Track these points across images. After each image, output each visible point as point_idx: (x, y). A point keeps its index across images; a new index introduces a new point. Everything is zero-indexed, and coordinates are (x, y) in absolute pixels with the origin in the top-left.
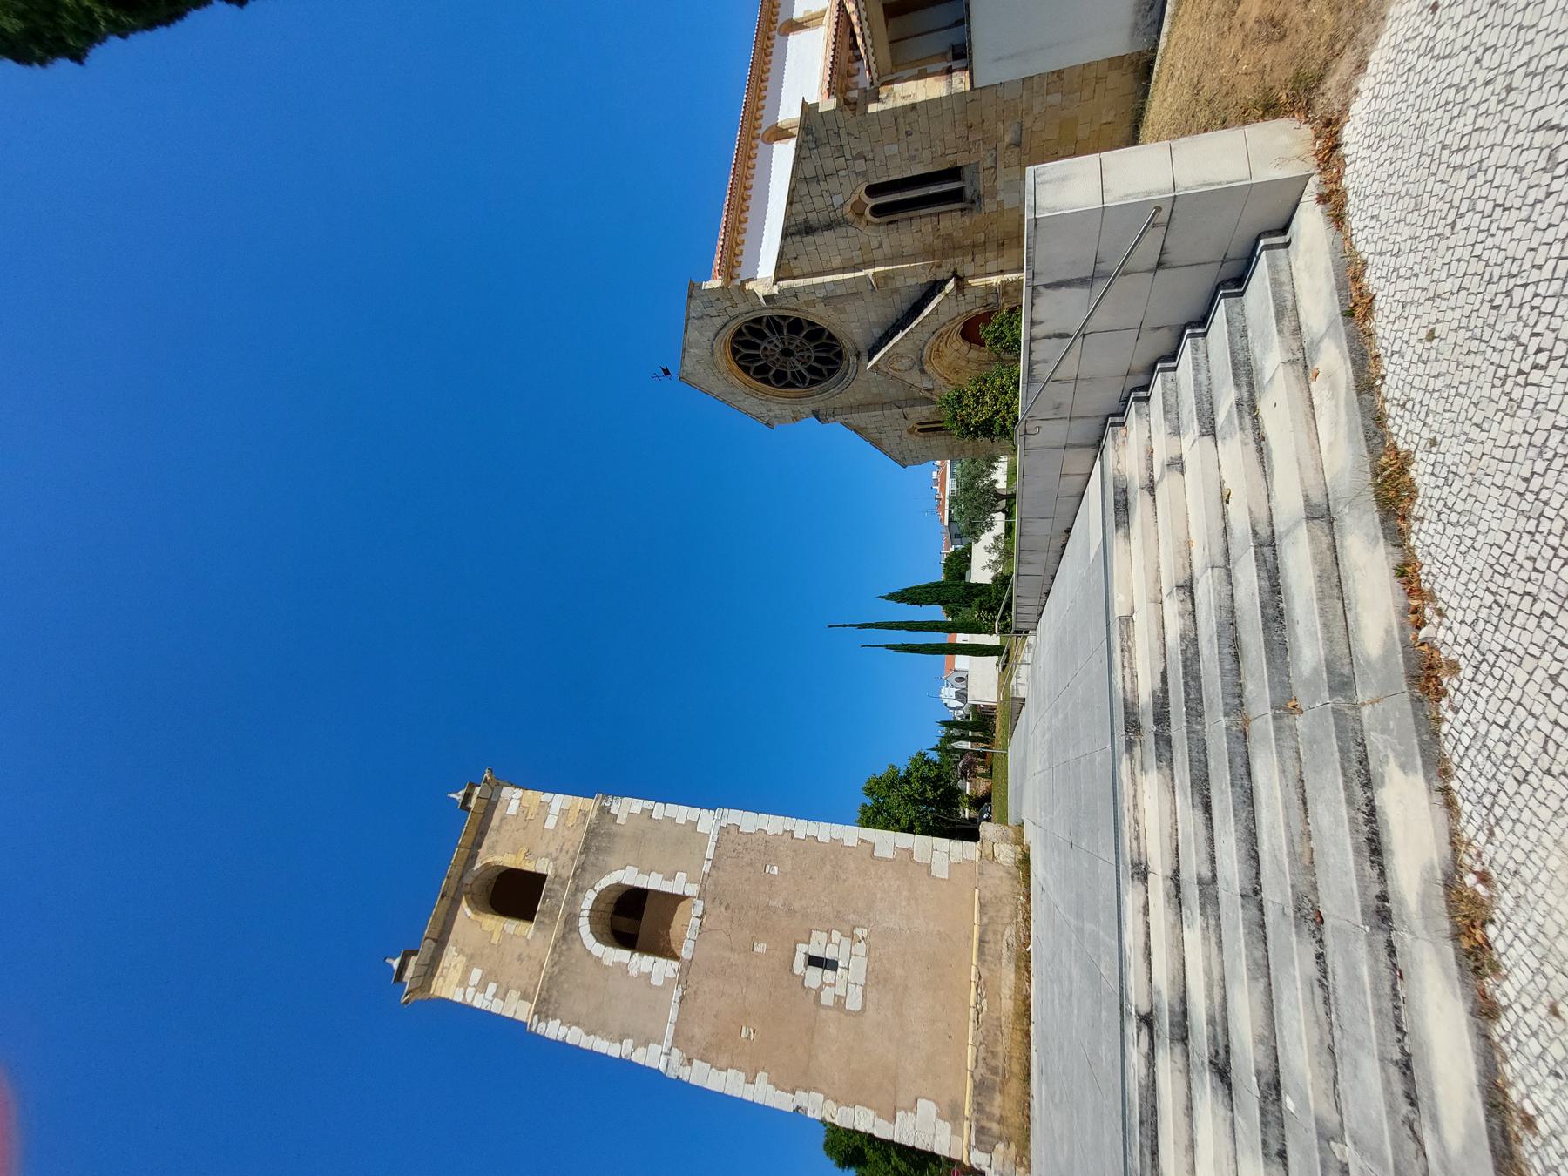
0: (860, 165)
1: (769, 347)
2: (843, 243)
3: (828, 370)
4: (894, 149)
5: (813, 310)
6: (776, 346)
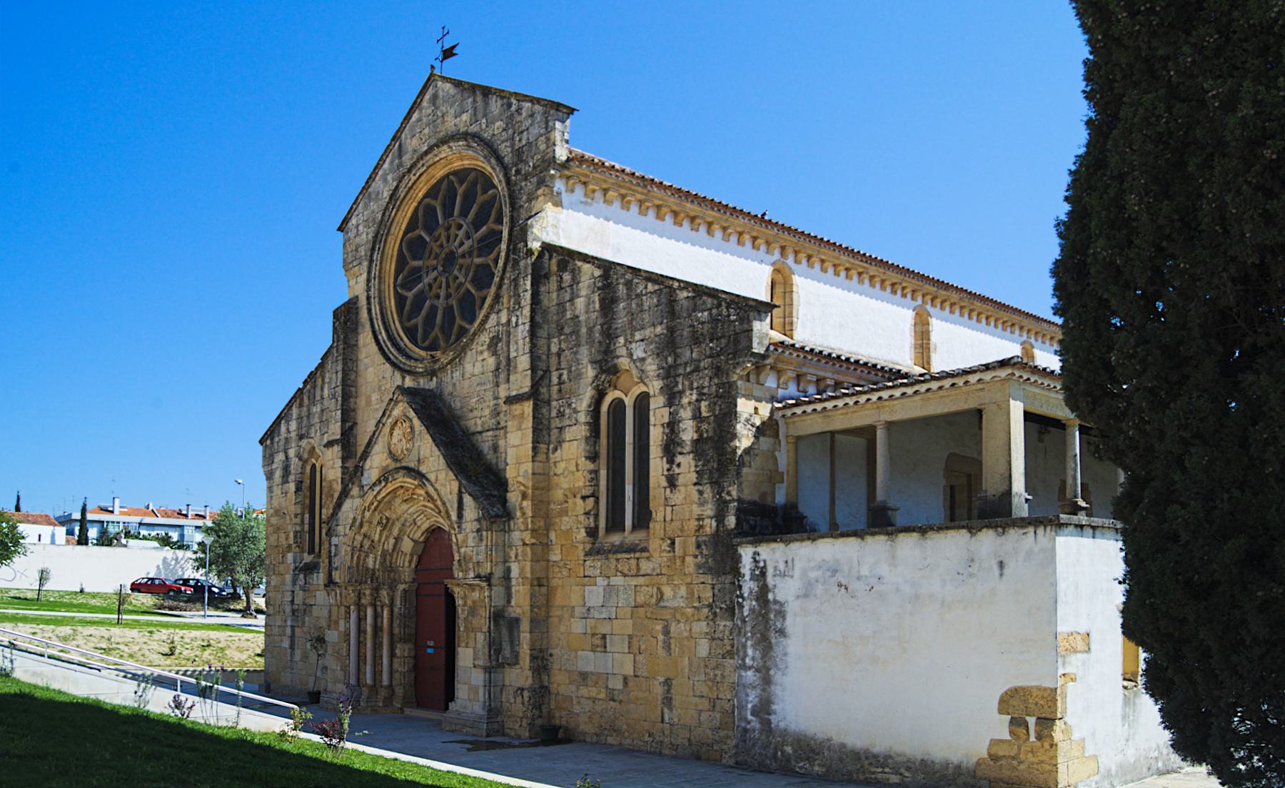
1: (461, 233)
3: (416, 327)
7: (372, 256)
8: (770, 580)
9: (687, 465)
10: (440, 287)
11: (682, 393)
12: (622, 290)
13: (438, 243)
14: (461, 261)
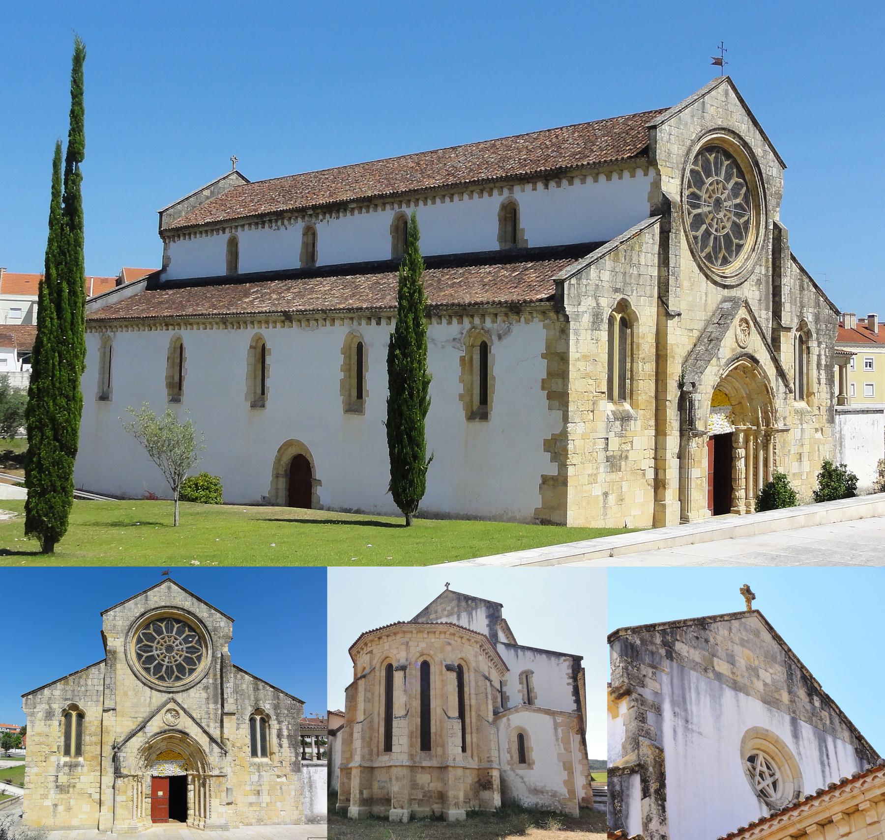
6: (177, 646)
7: (128, 632)
8: (311, 774)
9: (285, 742)
10: (165, 657)
11: (282, 721)
12: (261, 687)
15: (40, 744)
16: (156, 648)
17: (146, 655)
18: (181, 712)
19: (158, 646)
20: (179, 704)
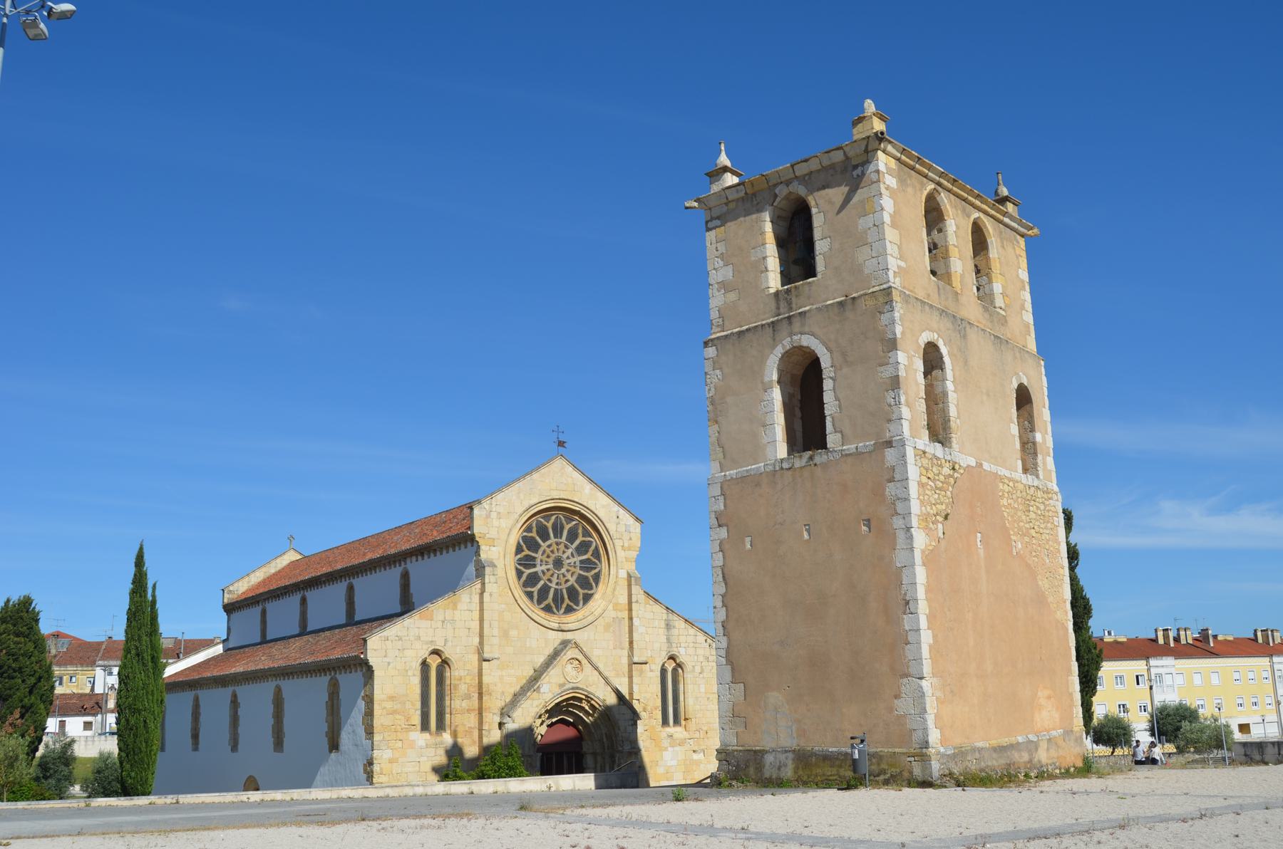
0: (698, 669)
2: (657, 646)
4: (703, 690)
5: (611, 607)
6: (568, 558)
10: (552, 575)
13: (551, 549)
14: (570, 568)
15: (394, 712)
16: (541, 561)
17: (528, 571)
18: (584, 661)
19: (544, 558)
20: (581, 651)
